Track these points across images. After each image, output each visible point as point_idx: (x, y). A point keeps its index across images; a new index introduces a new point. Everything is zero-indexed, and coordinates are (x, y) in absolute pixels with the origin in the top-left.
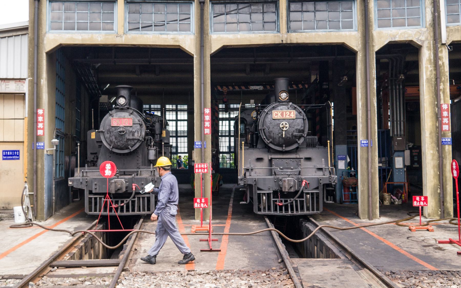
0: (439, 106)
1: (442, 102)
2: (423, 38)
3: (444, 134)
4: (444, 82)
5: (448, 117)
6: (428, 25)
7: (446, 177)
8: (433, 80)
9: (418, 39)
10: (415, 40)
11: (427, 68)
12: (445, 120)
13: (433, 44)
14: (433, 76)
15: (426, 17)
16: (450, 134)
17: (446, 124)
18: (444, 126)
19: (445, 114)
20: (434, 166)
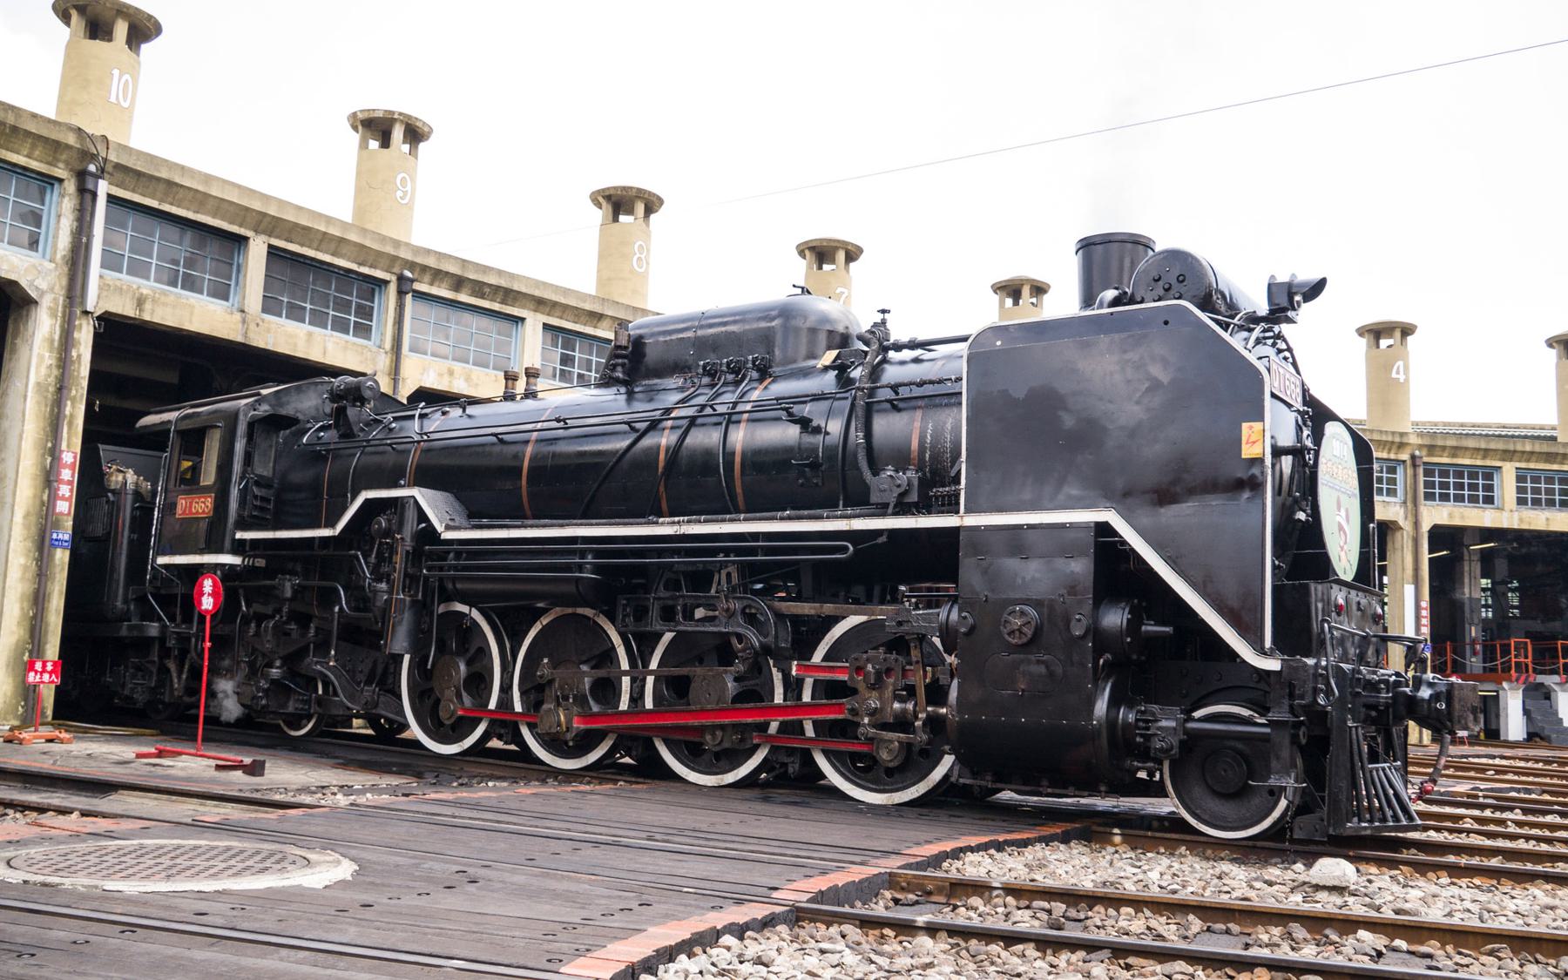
0: (54, 453)
1: (64, 446)
2: (44, 286)
3: (58, 521)
4: (73, 400)
5: (70, 483)
6: (59, 257)
7: (47, 625)
8: (51, 389)
9: (31, 283)
10: (24, 283)
11: (41, 357)
12: (65, 490)
13: (64, 307)
14: (52, 380)
15: (56, 237)
16: (69, 523)
17: (63, 498)
18: (59, 503)
19: (66, 474)
20: (23, 595)
